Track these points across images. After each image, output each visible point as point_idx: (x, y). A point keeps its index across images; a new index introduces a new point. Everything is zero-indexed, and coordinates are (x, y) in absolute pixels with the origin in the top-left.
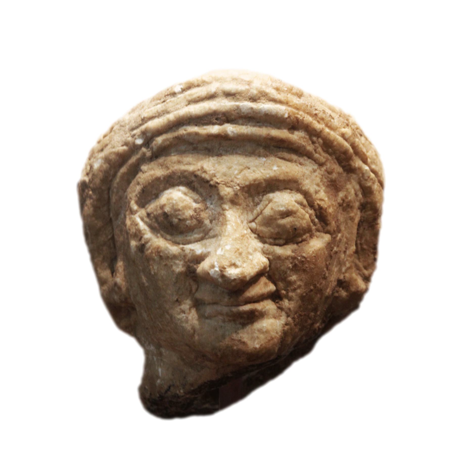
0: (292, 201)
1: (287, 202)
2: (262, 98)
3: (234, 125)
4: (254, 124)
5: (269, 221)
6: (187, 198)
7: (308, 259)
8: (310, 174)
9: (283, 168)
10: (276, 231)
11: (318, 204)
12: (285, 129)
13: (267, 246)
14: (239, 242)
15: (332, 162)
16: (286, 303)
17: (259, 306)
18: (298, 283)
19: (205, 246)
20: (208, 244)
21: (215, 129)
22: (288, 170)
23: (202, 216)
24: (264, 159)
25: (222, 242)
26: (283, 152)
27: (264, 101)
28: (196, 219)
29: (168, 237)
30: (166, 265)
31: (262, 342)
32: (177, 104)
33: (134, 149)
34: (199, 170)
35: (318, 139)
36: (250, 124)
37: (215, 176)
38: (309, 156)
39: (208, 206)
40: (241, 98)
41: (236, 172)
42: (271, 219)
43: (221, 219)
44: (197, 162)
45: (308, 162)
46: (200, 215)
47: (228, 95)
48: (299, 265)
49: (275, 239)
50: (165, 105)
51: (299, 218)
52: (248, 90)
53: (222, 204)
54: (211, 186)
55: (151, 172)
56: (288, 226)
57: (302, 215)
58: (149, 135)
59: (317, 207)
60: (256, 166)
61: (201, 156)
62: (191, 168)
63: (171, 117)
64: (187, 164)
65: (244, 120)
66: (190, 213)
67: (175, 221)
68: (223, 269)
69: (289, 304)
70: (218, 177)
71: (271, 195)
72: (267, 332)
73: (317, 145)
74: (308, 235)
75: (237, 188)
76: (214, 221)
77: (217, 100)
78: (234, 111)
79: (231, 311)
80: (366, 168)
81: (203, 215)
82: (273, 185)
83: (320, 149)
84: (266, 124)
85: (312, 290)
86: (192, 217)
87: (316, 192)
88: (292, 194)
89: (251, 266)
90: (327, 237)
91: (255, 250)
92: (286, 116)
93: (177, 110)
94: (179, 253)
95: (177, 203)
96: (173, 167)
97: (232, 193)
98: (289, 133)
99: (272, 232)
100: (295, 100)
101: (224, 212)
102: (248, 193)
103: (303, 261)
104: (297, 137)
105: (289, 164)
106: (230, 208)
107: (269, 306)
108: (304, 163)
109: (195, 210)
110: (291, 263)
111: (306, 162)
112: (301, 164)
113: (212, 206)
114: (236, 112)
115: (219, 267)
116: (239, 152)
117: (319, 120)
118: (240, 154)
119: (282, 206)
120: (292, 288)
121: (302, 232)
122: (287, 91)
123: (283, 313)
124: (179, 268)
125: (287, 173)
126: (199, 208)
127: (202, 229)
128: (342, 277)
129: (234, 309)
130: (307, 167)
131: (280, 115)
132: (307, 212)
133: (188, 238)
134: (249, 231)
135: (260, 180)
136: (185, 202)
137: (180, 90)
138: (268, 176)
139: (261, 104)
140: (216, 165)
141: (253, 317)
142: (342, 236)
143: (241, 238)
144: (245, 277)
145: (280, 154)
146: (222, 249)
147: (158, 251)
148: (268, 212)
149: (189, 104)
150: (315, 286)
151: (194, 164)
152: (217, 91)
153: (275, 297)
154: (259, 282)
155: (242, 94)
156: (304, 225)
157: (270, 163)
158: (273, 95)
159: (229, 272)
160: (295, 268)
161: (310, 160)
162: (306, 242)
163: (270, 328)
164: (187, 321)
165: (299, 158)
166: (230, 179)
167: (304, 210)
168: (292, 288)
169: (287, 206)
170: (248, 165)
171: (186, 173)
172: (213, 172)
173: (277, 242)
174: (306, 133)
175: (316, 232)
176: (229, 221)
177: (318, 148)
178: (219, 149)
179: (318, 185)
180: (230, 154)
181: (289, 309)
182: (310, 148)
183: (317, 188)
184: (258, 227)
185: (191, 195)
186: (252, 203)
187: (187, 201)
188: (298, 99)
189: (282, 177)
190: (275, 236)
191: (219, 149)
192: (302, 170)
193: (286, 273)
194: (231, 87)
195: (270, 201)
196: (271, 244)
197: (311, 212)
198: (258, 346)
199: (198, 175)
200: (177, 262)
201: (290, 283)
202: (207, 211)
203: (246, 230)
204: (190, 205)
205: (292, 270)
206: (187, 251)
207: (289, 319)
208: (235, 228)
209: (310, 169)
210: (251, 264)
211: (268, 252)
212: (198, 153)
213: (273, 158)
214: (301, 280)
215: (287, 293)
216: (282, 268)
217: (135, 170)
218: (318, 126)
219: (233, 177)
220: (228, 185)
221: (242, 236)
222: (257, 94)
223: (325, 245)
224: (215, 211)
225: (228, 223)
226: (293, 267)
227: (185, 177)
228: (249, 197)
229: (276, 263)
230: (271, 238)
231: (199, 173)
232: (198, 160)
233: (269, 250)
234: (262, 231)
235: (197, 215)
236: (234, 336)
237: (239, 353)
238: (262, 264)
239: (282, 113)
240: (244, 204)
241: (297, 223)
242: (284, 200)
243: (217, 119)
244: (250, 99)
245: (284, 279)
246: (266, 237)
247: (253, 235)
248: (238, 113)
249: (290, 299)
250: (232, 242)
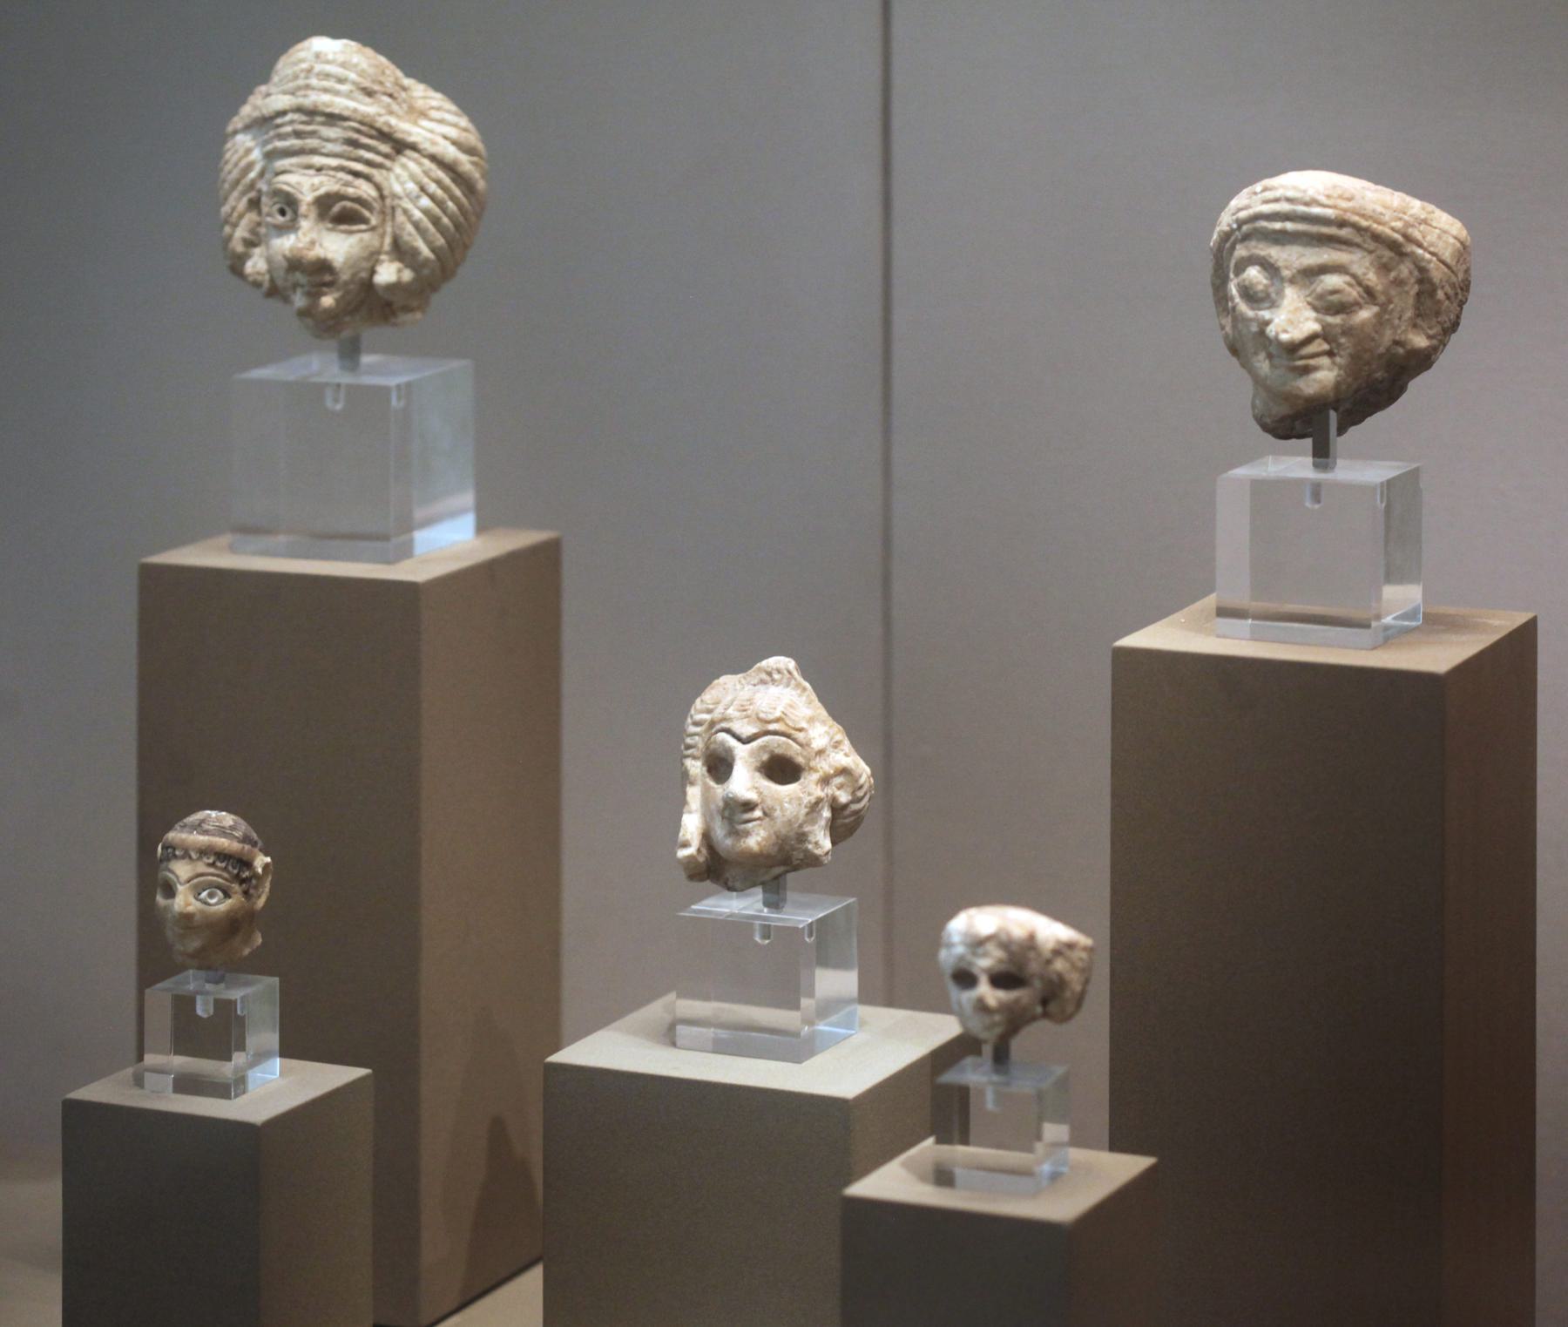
5: (1321, 297)
16: (1338, 359)
17: (1312, 362)
21: (1278, 226)
33: (1232, 231)
38: (1358, 246)
47: (1289, 200)
48: (1347, 331)
55: (1241, 252)
62: (1262, 253)
63: (1251, 212)
66: (1260, 287)
72: (1320, 381)
81: (1271, 290)
82: (1324, 269)
90: (1376, 309)
100: (1344, 204)
104: (1344, 233)
107: (1325, 361)
124: (1254, 328)
141: (1307, 370)
147: (1242, 314)
148: (1319, 290)
153: (1330, 354)
160: (1344, 333)
182: (1358, 240)
194: (1290, 194)
201: (1339, 345)
217: (1233, 248)
218: (1364, 223)
237: (1297, 397)
242: (1333, 281)
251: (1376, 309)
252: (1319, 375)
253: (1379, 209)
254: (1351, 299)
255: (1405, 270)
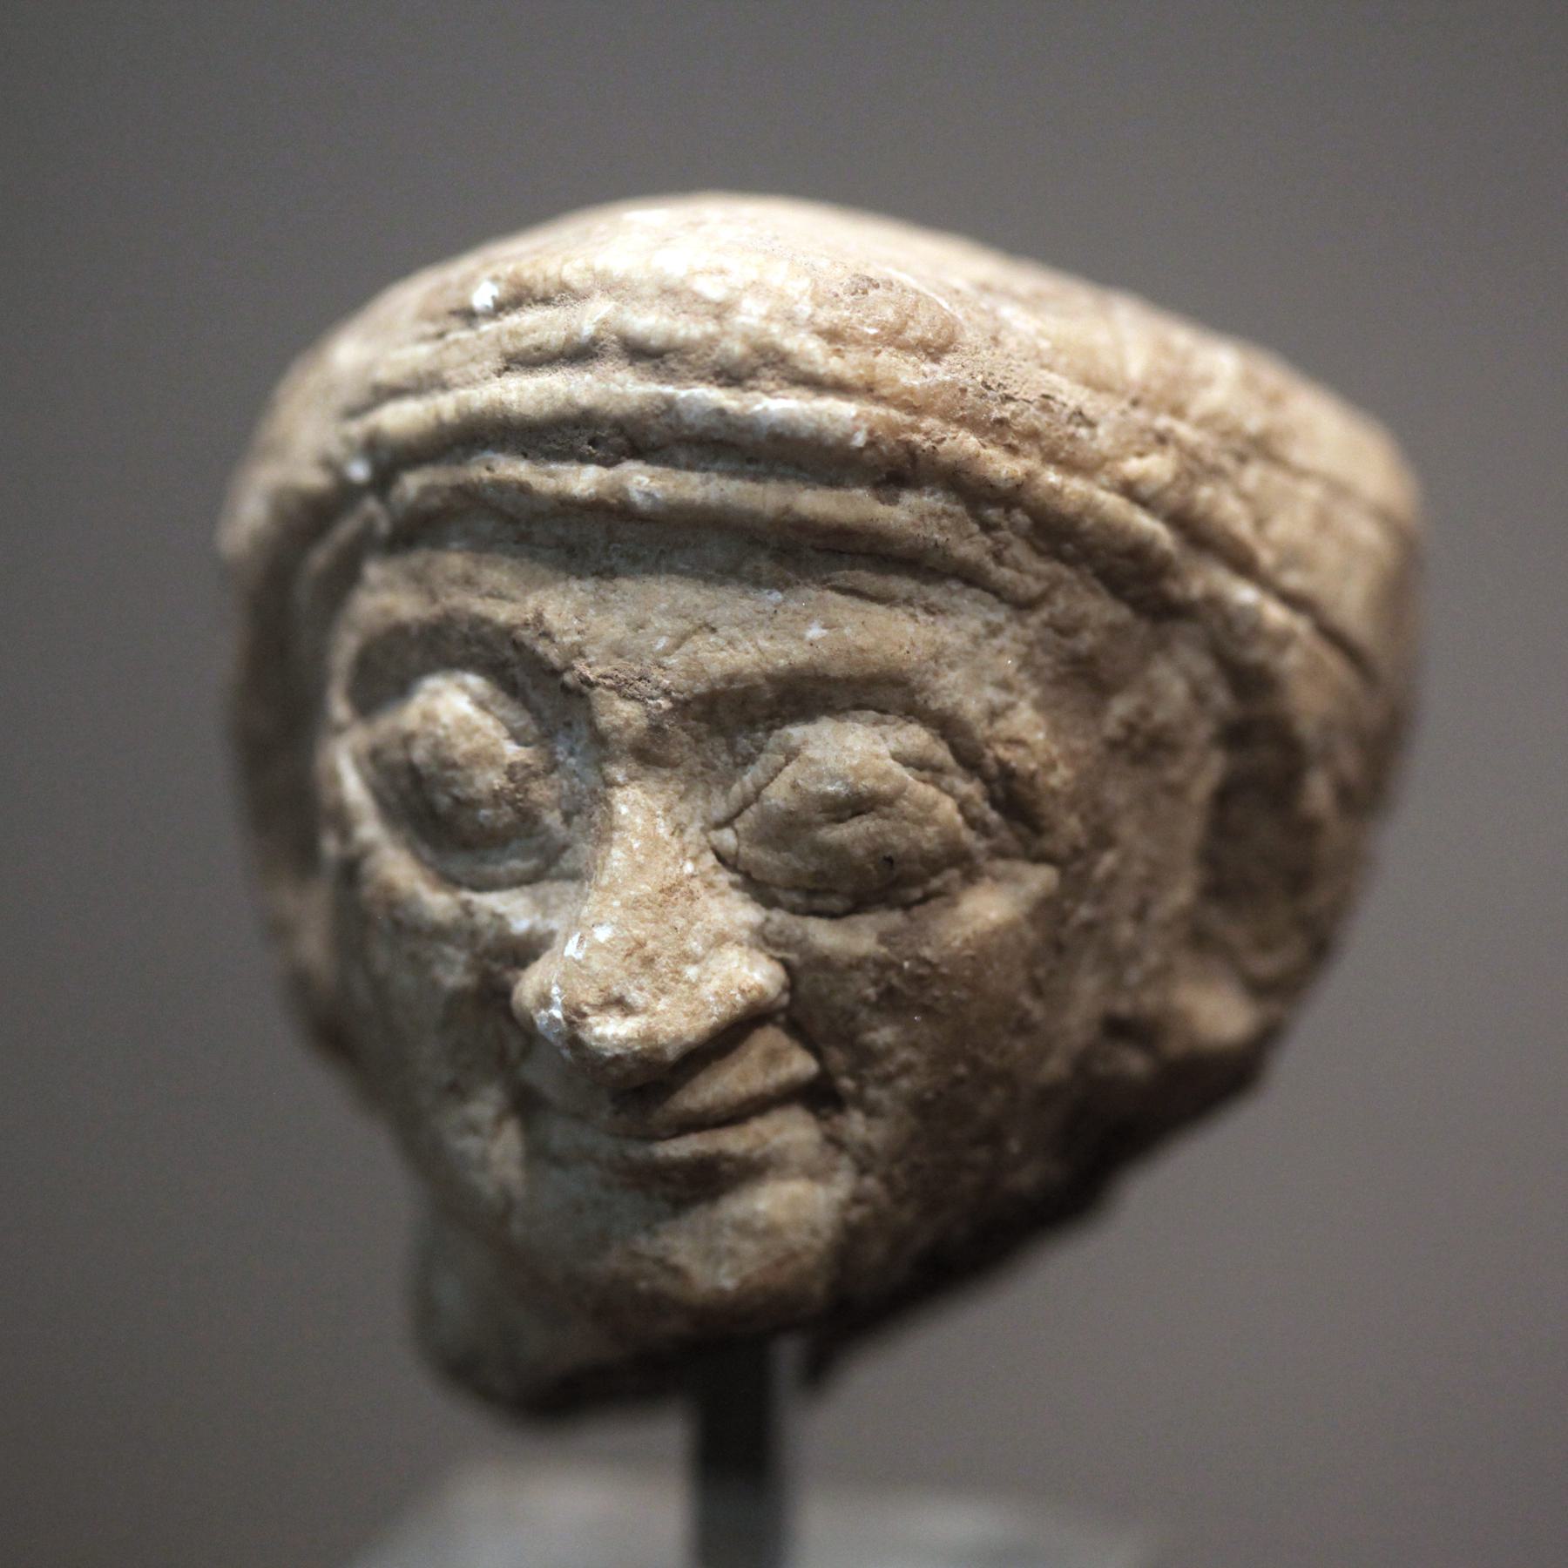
0: (877, 756)
1: (855, 762)
2: (765, 372)
3: (659, 469)
4: (734, 466)
5: (785, 830)
6: (487, 723)
7: (944, 970)
8: (969, 647)
9: (847, 631)
10: (812, 869)
11: (1001, 763)
12: (859, 485)
13: (778, 917)
14: (647, 914)
15: (1079, 589)
16: (855, 1125)
17: (734, 1141)
18: (904, 1055)
19: (543, 905)
20: (553, 900)
21: (583, 480)
22: (865, 640)
23: (534, 796)
24: (777, 596)
25: (585, 911)
26: (852, 568)
27: (772, 385)
28: (513, 803)
29: (426, 852)
30: (413, 957)
31: (749, 1270)
32: (473, 360)
33: (344, 495)
34: (526, 625)
35: (1008, 511)
36: (719, 465)
37: (582, 654)
38: (970, 577)
39: (561, 758)
40: (682, 369)
41: (662, 643)
42: (791, 825)
43: (597, 818)
44: (525, 593)
45: (966, 599)
46: (527, 790)
47: (639, 353)
48: (904, 990)
49: (811, 893)
50: (438, 353)
51: (905, 818)
52: (712, 341)
53: (605, 759)
54: (565, 688)
55: (387, 597)
56: (859, 852)
57: (919, 806)
58: (385, 456)
59: (994, 770)
60: (742, 624)
61: (543, 571)
62: (503, 613)
63: (446, 405)
64: (491, 595)
65: (695, 450)
66: (496, 779)
67: (443, 801)
68: (576, 1015)
69: (869, 1129)
70: (592, 659)
71: (796, 733)
72: (772, 1231)
73: (1005, 534)
74: (954, 874)
75: (659, 707)
76: (576, 819)
77: (602, 368)
78: (657, 416)
79: (625, 1158)
80: (1245, 594)
81: (541, 792)
82: (808, 694)
83: (1019, 550)
84: (781, 470)
85: (960, 1081)
86: (497, 797)
87: (994, 714)
88: (884, 727)
89: (687, 1008)
90: (1040, 879)
91: (721, 939)
92: (860, 440)
93: (468, 383)
94: (456, 920)
95: (448, 738)
96: (448, 596)
97: (643, 723)
98: (879, 499)
99: (795, 871)
100: (912, 374)
101: (610, 791)
102: (708, 722)
103: (921, 978)
104: (906, 514)
105: (878, 613)
106: (632, 778)
107: (793, 1131)
108: (944, 606)
109: (511, 771)
110: (875, 983)
111: (956, 599)
112: (929, 610)
113: (572, 761)
114: (663, 420)
115: (565, 1006)
116: (681, 566)
117: (1015, 442)
118: (681, 573)
119: (834, 777)
120: (878, 1071)
121: (918, 868)
122: (875, 337)
123: (845, 1161)
124: (455, 974)
125: (861, 650)
126: (527, 766)
127: (534, 843)
128: (1123, 1006)
129: (636, 1152)
130: (960, 621)
131: (830, 441)
132: (950, 792)
133: (489, 869)
134: (710, 859)
135: (751, 676)
136: (477, 736)
137: (490, 303)
138: (782, 662)
139: (757, 394)
140: (592, 612)
141: (711, 1180)
142: (1125, 860)
143: (660, 897)
144: (659, 1050)
145: (842, 576)
146: (581, 941)
147: (392, 901)
148: (778, 794)
149: (507, 369)
150: (975, 1063)
151: (513, 600)
152: (602, 334)
153: (817, 1096)
154: (743, 1048)
155: (688, 353)
156: (926, 845)
157: (795, 613)
158: (811, 363)
159: (598, 1031)
160: (891, 1002)
161: (976, 592)
162: (945, 900)
163: (782, 1215)
164: (484, 1163)
165: (924, 587)
166: (637, 668)
167: (936, 784)
168: (878, 1071)
169: (851, 780)
170: (710, 618)
171: (486, 629)
172: (577, 638)
173: (818, 903)
174: (953, 497)
175: (990, 859)
176: (621, 828)
177: (1008, 545)
178: (606, 549)
179: (1005, 685)
180: (644, 572)
181: (867, 1147)
182: (971, 548)
183: (998, 697)
184: (744, 850)
185: (501, 712)
186: (724, 757)
187: (485, 735)
188: (927, 367)
189: (837, 669)
190: (810, 885)
191: (606, 549)
192: (930, 635)
193: (853, 1017)
194: (648, 322)
195: (792, 754)
196: (794, 910)
197: (969, 788)
198: (729, 1283)
199: (522, 644)
200: (449, 950)
201: (866, 1057)
202: (555, 776)
203: (695, 859)
204: (493, 750)
205: (876, 1007)
206: (483, 919)
207: (870, 1182)
208: (641, 858)
209: (975, 625)
210: (689, 1001)
211: (782, 939)
212: (533, 556)
213: (812, 593)
214: (914, 1045)
215: (861, 1087)
216: (839, 999)
217: (346, 576)
218: (1003, 466)
219: (648, 661)
220: (630, 691)
221: (662, 891)
222: (744, 359)
223: (1025, 908)
224: (582, 781)
225: (616, 835)
226: (880, 996)
227: (482, 641)
228: (711, 733)
229: (816, 980)
230: (795, 888)
231: (526, 635)
232: (531, 584)
233: (787, 932)
234: (757, 864)
235: (517, 790)
236: (642, 1243)
237: (658, 1304)
238: (738, 997)
239: (839, 434)
240: (694, 762)
241: (894, 839)
242: (848, 751)
243: (593, 442)
244: (717, 375)
245: (849, 1039)
246: (776, 886)
247: (724, 878)
248: (670, 427)
249: (872, 1111)
250: (620, 912)
251: (1040, 879)
252: (769, 1201)
253: (1072, 395)
254: (928, 838)
255: (1174, 683)
